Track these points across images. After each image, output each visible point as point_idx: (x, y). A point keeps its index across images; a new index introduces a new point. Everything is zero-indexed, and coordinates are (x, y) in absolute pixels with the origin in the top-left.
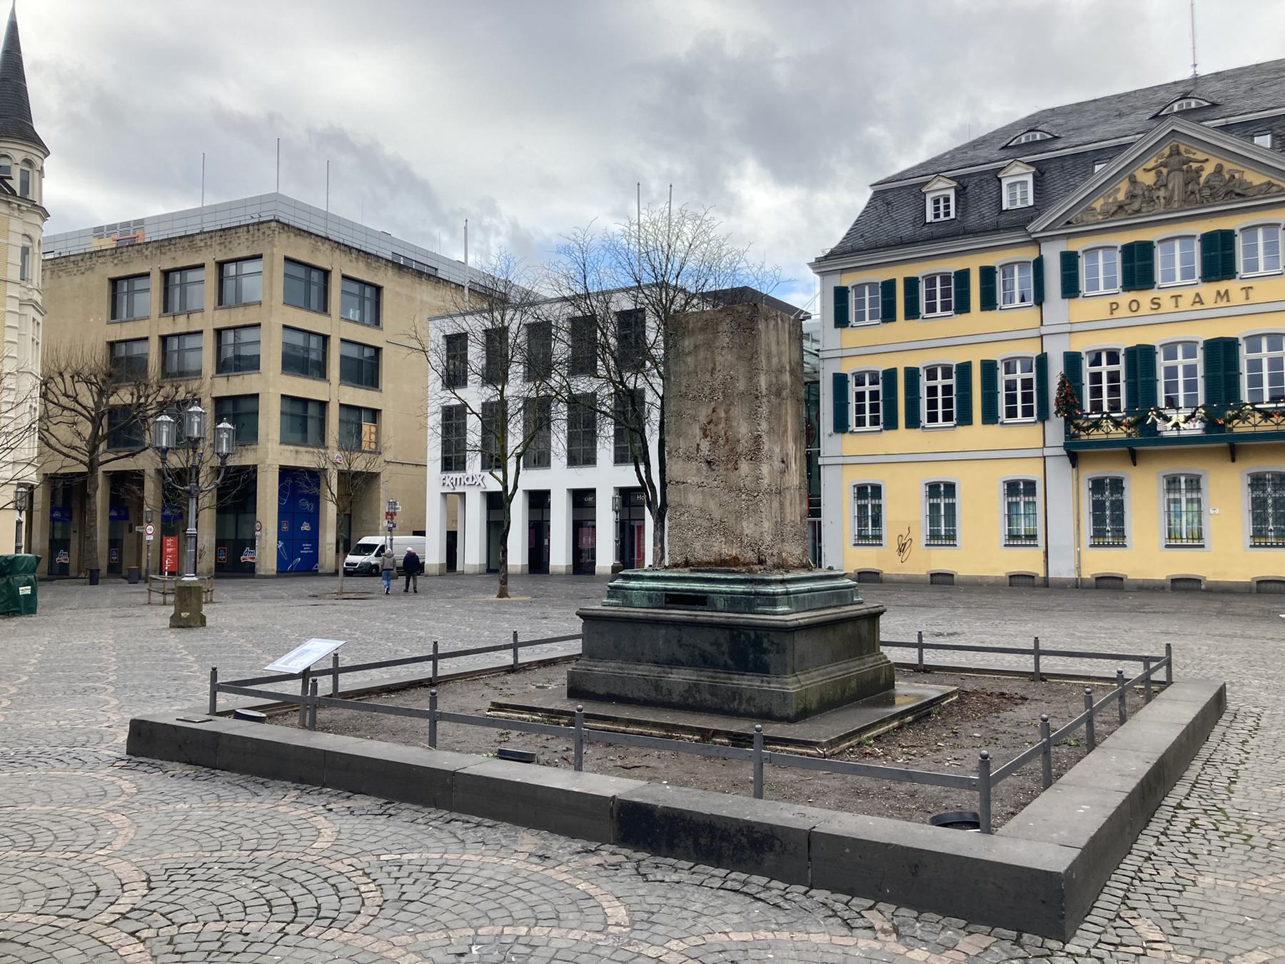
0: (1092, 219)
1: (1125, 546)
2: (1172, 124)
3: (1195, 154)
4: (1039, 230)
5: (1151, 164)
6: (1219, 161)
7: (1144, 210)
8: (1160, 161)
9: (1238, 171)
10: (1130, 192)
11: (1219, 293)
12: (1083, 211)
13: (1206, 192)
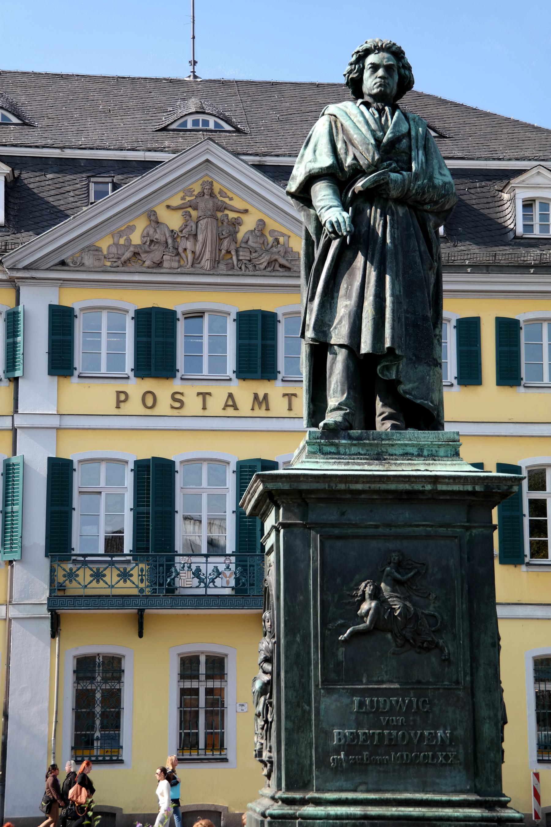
0: (97, 263)
1: (121, 762)
2: (207, 151)
3: (231, 199)
4: (20, 266)
5: (176, 202)
6: (262, 217)
7: (166, 264)
8: (188, 199)
9: (283, 235)
10: (148, 235)
11: (256, 396)
12: (83, 249)
13: (244, 255)
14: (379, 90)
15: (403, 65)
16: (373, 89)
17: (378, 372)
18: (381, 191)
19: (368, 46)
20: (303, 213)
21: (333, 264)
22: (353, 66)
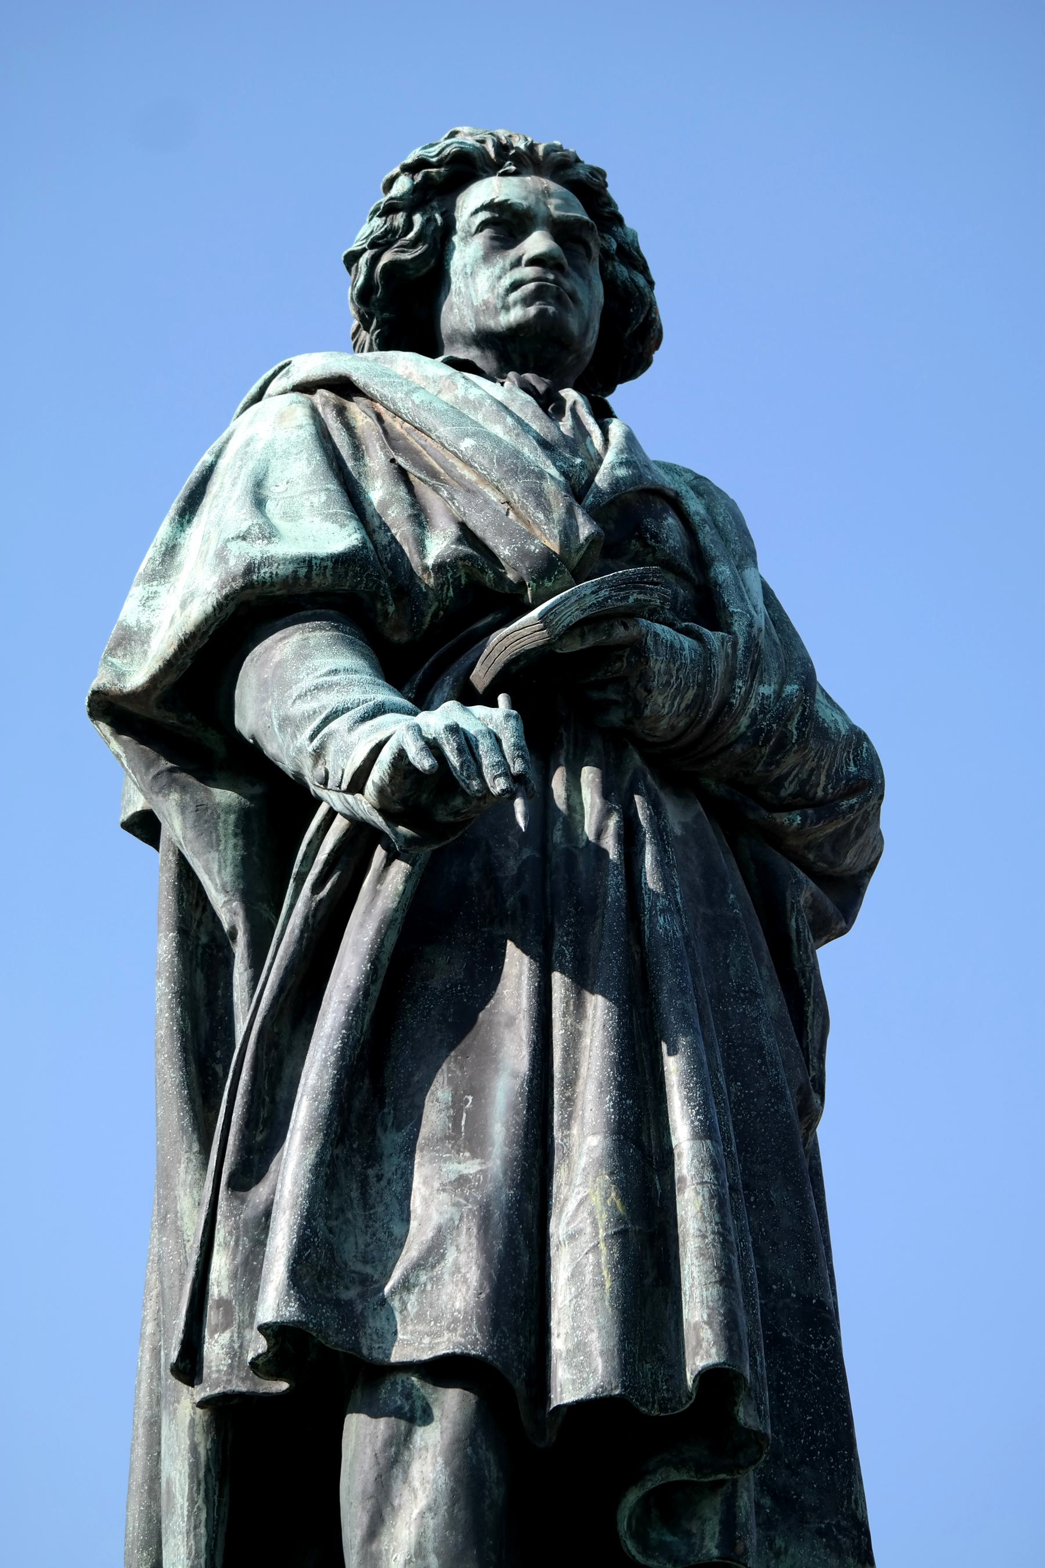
14: (532, 310)
15: (619, 246)
16: (506, 308)
17: (623, 1526)
18: (602, 686)
19: (467, 137)
20: (175, 796)
21: (375, 991)
22: (399, 219)
